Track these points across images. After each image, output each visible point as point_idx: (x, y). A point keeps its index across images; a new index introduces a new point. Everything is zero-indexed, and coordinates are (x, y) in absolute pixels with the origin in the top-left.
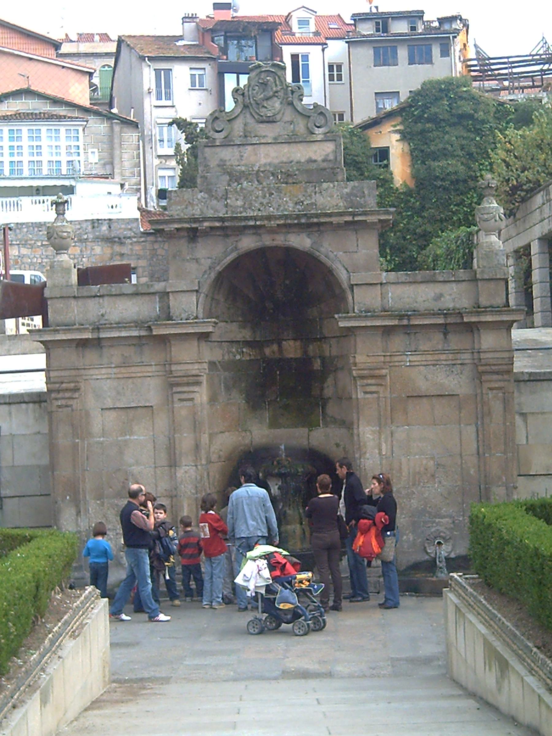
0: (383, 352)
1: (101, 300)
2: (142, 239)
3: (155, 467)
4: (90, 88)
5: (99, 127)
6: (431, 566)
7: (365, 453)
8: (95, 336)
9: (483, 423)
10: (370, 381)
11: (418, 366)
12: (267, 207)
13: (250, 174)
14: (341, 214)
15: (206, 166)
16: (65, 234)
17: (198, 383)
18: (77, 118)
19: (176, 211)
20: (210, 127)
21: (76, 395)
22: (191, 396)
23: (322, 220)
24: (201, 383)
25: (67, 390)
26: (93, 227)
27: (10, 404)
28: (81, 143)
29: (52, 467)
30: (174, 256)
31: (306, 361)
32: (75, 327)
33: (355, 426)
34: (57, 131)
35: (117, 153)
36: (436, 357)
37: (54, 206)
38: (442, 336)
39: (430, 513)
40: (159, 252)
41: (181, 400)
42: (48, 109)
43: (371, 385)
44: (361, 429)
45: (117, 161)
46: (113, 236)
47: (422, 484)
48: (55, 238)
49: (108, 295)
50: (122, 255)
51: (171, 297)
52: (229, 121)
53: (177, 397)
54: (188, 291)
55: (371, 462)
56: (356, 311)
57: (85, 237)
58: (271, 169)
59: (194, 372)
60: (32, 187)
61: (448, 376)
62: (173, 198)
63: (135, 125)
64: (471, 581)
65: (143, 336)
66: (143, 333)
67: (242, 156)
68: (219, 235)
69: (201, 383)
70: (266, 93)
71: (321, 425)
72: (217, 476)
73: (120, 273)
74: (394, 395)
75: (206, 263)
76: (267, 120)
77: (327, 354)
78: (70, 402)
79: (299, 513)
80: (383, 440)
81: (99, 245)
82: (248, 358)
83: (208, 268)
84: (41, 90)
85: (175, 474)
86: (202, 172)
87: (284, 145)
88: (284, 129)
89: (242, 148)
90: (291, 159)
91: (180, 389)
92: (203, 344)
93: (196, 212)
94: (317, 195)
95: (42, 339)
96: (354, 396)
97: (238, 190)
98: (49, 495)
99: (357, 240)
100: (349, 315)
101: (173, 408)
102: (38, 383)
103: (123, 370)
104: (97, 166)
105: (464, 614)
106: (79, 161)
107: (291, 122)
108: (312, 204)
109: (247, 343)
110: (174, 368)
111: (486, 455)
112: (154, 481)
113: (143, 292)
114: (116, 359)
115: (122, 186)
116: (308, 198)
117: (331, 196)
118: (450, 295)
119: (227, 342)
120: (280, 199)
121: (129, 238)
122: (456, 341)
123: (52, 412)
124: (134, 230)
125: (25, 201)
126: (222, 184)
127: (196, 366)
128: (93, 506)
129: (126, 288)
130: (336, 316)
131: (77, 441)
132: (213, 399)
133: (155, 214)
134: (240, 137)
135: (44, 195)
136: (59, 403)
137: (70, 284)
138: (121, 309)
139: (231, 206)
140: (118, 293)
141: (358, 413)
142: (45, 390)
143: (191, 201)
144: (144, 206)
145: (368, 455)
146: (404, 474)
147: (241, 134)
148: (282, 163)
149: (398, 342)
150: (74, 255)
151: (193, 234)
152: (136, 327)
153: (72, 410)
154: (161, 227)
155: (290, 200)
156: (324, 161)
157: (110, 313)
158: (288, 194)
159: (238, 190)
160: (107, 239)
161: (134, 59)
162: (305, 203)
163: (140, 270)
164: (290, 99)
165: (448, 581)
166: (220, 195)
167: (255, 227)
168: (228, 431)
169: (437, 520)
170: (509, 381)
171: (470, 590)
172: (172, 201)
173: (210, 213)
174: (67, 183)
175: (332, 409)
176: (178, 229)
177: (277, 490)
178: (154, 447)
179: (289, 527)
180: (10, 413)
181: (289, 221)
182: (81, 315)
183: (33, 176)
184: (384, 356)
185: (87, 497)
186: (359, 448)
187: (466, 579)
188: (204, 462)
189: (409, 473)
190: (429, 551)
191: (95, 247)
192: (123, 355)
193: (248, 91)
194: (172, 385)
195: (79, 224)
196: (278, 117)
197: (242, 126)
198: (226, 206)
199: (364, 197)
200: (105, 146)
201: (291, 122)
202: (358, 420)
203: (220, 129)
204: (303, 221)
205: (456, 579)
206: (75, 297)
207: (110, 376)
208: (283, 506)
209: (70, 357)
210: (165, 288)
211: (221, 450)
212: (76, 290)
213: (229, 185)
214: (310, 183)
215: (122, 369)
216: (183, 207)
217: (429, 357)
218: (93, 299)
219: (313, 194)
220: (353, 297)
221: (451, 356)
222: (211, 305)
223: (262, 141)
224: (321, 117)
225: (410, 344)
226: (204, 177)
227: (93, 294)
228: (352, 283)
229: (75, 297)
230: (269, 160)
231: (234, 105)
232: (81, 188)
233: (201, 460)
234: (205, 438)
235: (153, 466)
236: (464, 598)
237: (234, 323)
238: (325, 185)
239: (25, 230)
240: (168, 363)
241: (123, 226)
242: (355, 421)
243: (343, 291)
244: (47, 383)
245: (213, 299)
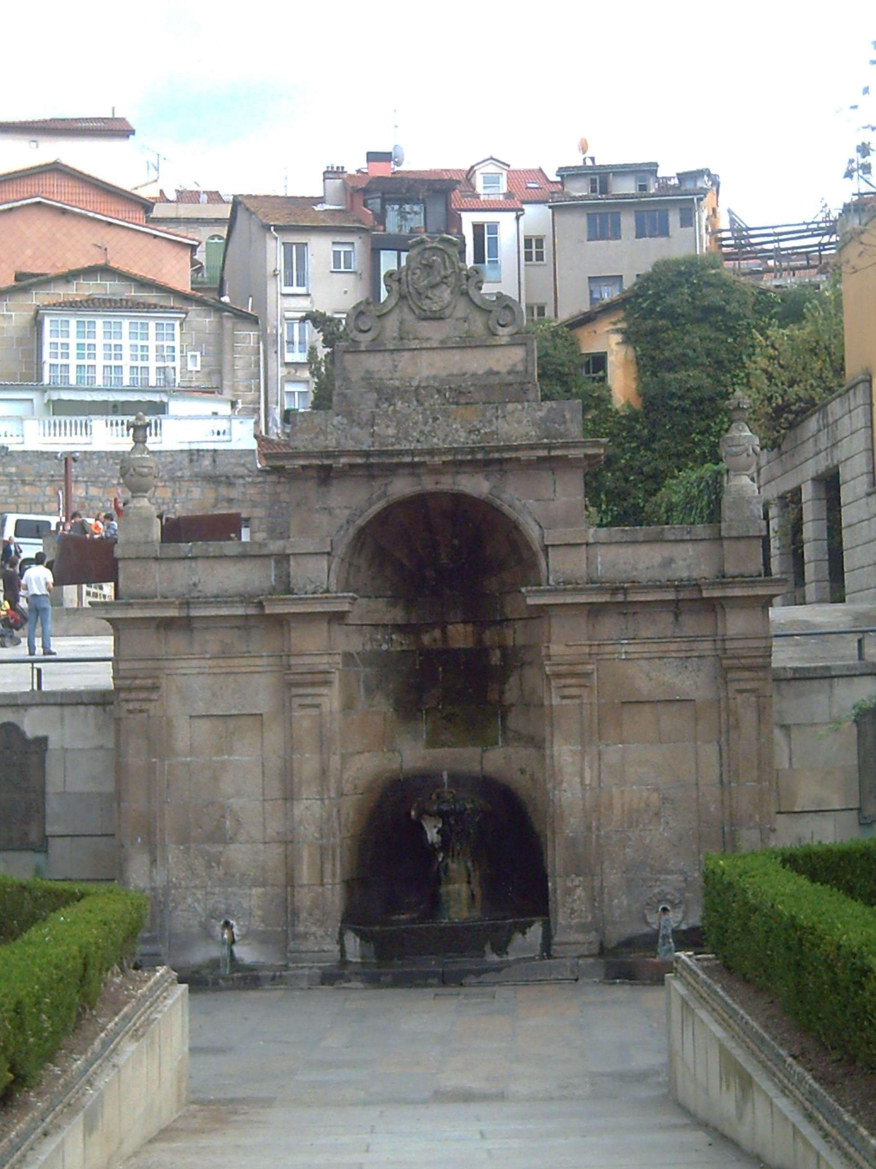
0: (589, 639)
1: (193, 564)
2: (260, 479)
3: (264, 800)
4: (192, 267)
5: (203, 321)
6: (650, 942)
7: (561, 782)
8: (183, 614)
9: (728, 740)
10: (569, 681)
11: (638, 659)
12: (430, 437)
13: (406, 391)
14: (531, 447)
15: (346, 379)
16: (146, 470)
17: (327, 683)
18: (172, 308)
19: (302, 442)
20: (352, 324)
21: (155, 696)
22: (317, 701)
23: (506, 455)
24: (331, 682)
25: (141, 688)
26: (191, 461)
27: (62, 705)
28: (177, 344)
29: (118, 796)
30: (298, 505)
31: (480, 652)
32: (156, 600)
33: (547, 745)
34: (145, 326)
35: (227, 357)
36: (663, 647)
37: (132, 431)
38: (671, 618)
39: (652, 868)
40: (284, 497)
41: (303, 706)
42: (133, 294)
43: (570, 686)
44: (555, 748)
45: (227, 369)
46: (218, 473)
47: (641, 826)
48: (132, 475)
49: (203, 557)
50: (230, 501)
51: (292, 563)
52: (379, 317)
53: (296, 702)
54: (316, 554)
55: (570, 795)
56: (551, 582)
57: (179, 474)
58: (436, 384)
59: (322, 668)
60: (107, 402)
61: (680, 673)
62: (299, 424)
63: (253, 320)
64: (705, 963)
65: (252, 615)
66: (251, 611)
67: (396, 366)
68: (361, 476)
69: (331, 682)
70: (430, 279)
71: (500, 743)
73: (224, 527)
74: (603, 701)
75: (342, 515)
76: (432, 316)
77: (510, 643)
78: (145, 706)
79: (467, 867)
80: (586, 764)
81: (198, 487)
82: (399, 649)
83: (345, 522)
84: (124, 269)
85: (292, 810)
86: (340, 388)
87: (454, 351)
88: (455, 329)
89: (396, 356)
90: (464, 370)
91: (301, 691)
92: (335, 627)
93: (331, 442)
94: (500, 420)
95: (109, 616)
96: (546, 703)
97: (390, 412)
98: (113, 835)
99: (555, 484)
100: (542, 588)
101: (291, 717)
102: (101, 677)
103: (222, 663)
104: (198, 374)
105: (693, 1010)
106: (174, 368)
107: (465, 320)
108: (493, 433)
109: (398, 628)
110: (293, 661)
111: (733, 785)
112: (262, 820)
113: (252, 553)
114: (213, 647)
115: (233, 404)
116: (487, 424)
117: (519, 422)
118: (685, 560)
119: (369, 625)
120: (448, 425)
121: (242, 477)
123: (120, 719)
124: (249, 466)
125: (98, 423)
126: (367, 405)
127: (325, 659)
129: (229, 547)
130: (523, 590)
131: (154, 760)
132: (348, 706)
133: (278, 444)
134: (394, 339)
135: (124, 415)
136: (131, 706)
137: (150, 540)
138: (222, 576)
139: (379, 435)
140: (217, 554)
141: (552, 725)
142: (113, 687)
143: (323, 428)
144: (263, 433)
145: (565, 785)
146: (615, 812)
147: (396, 335)
148: (452, 375)
149: (609, 626)
150: (164, 499)
151: (326, 475)
152: (242, 602)
153: (149, 716)
154: (281, 463)
155: (462, 427)
156: (509, 373)
157: (205, 582)
158: (459, 419)
159: (390, 412)
160: (210, 477)
161: (255, 229)
162: (482, 431)
163: (255, 523)
164: (465, 287)
165: (672, 963)
166: (365, 420)
167: (412, 465)
168: (369, 752)
169: (662, 877)
170: (765, 680)
171: (703, 976)
172: (297, 428)
173: (350, 445)
174: (156, 398)
175: (515, 721)
176: (303, 467)
177: (435, 835)
178: (263, 772)
179: (451, 887)
180: (62, 719)
181: (459, 457)
182: (165, 585)
183: (109, 387)
184: (590, 645)
185: (167, 842)
186: (553, 776)
187: (698, 960)
188: (333, 794)
189: (623, 811)
190: (650, 920)
191: (194, 489)
192: (222, 641)
193: (407, 275)
194: (291, 685)
195: (172, 455)
196: (447, 312)
197: (398, 324)
198: (372, 435)
199: (565, 422)
200: (211, 348)
201: (465, 320)
202: (552, 735)
203: (366, 328)
204: (479, 456)
205: (683, 961)
206: (156, 559)
207: (202, 670)
208: (443, 858)
209: (146, 643)
210: (285, 548)
211: (358, 778)
212: (158, 548)
213: (377, 406)
214: (490, 403)
215: (220, 660)
216: (312, 435)
217: (654, 647)
218: (182, 562)
219: (494, 419)
220: (547, 565)
221: (684, 646)
222: (348, 573)
223: (425, 345)
224: (507, 312)
225: (626, 628)
226: (343, 396)
227: (183, 554)
228: (546, 543)
229: (156, 559)
230: (433, 372)
231: (387, 294)
232: (176, 406)
233: (329, 790)
234: (335, 761)
235: (261, 798)
236: (694, 988)
237: (381, 599)
238: (510, 407)
239: (96, 462)
240: (283, 656)
241: (233, 461)
242: (548, 737)
243: (534, 555)
244: (114, 678)
245: (350, 565)
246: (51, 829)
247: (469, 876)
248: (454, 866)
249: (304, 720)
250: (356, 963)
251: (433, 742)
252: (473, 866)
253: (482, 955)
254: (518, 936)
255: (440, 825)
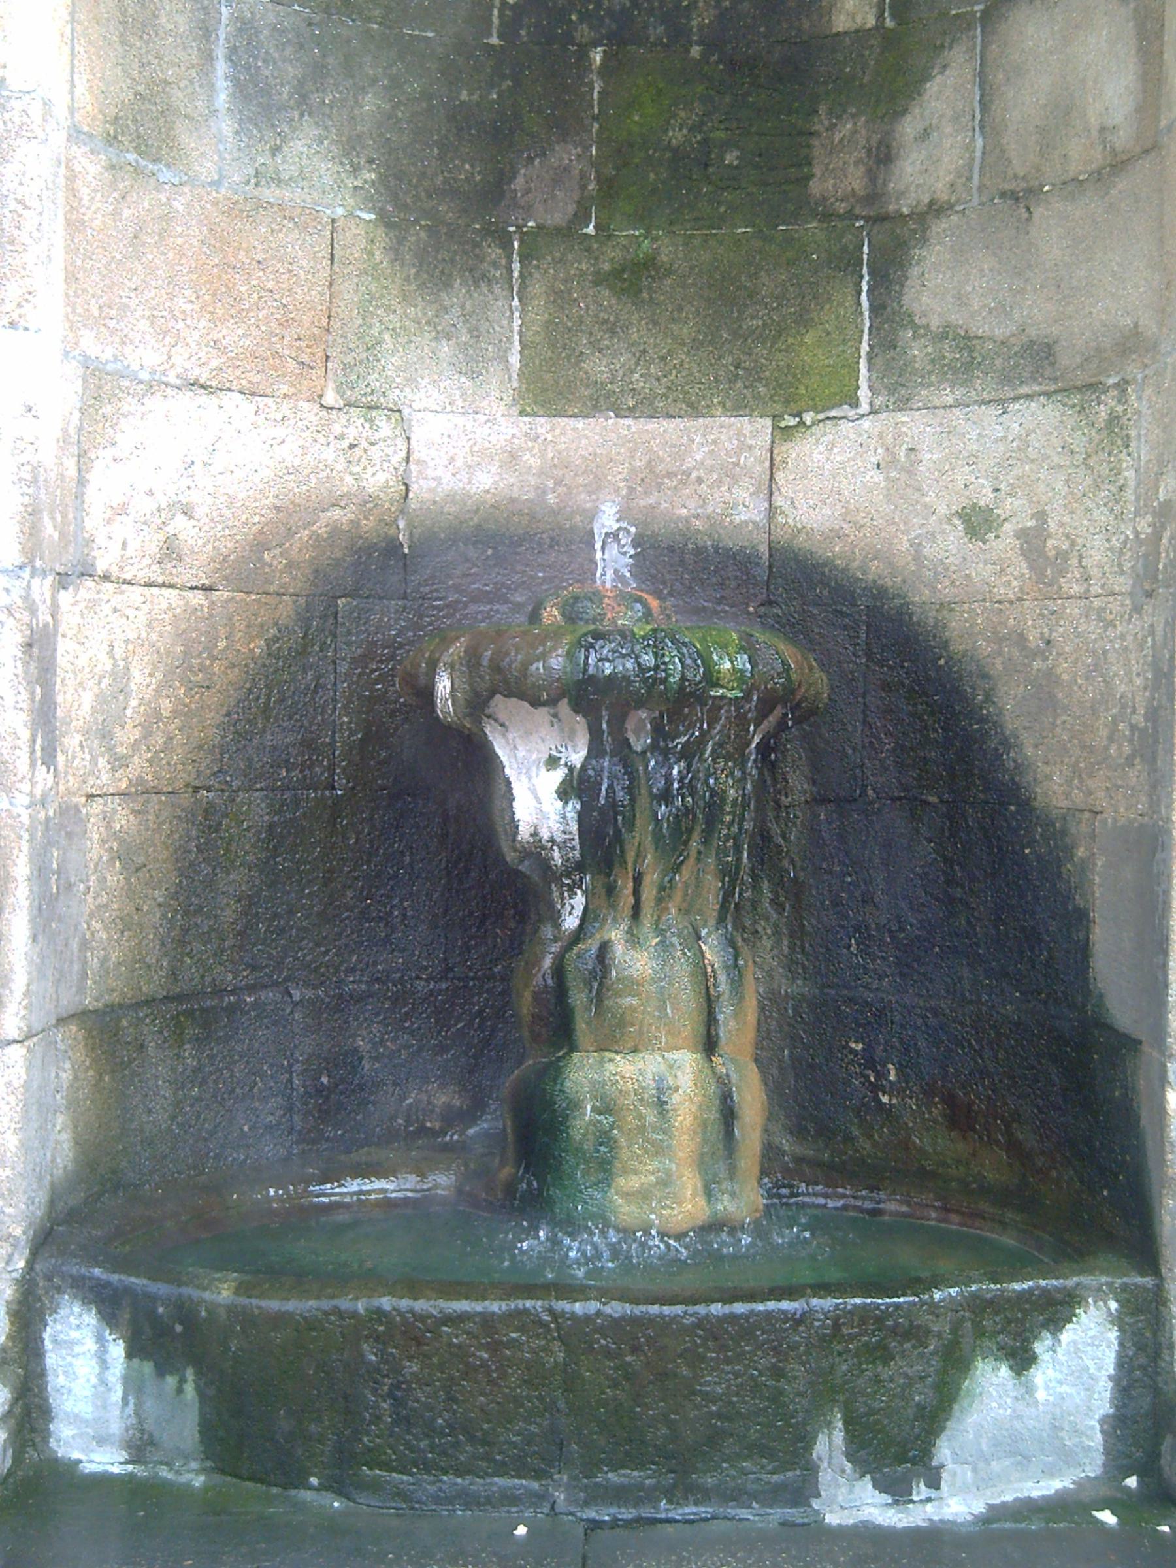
72: (141, 680)
247: (711, 1020)
248: (635, 961)
250: (103, 1480)
251: (550, 387)
252: (735, 970)
253: (803, 1490)
254: (991, 1380)
255: (577, 756)
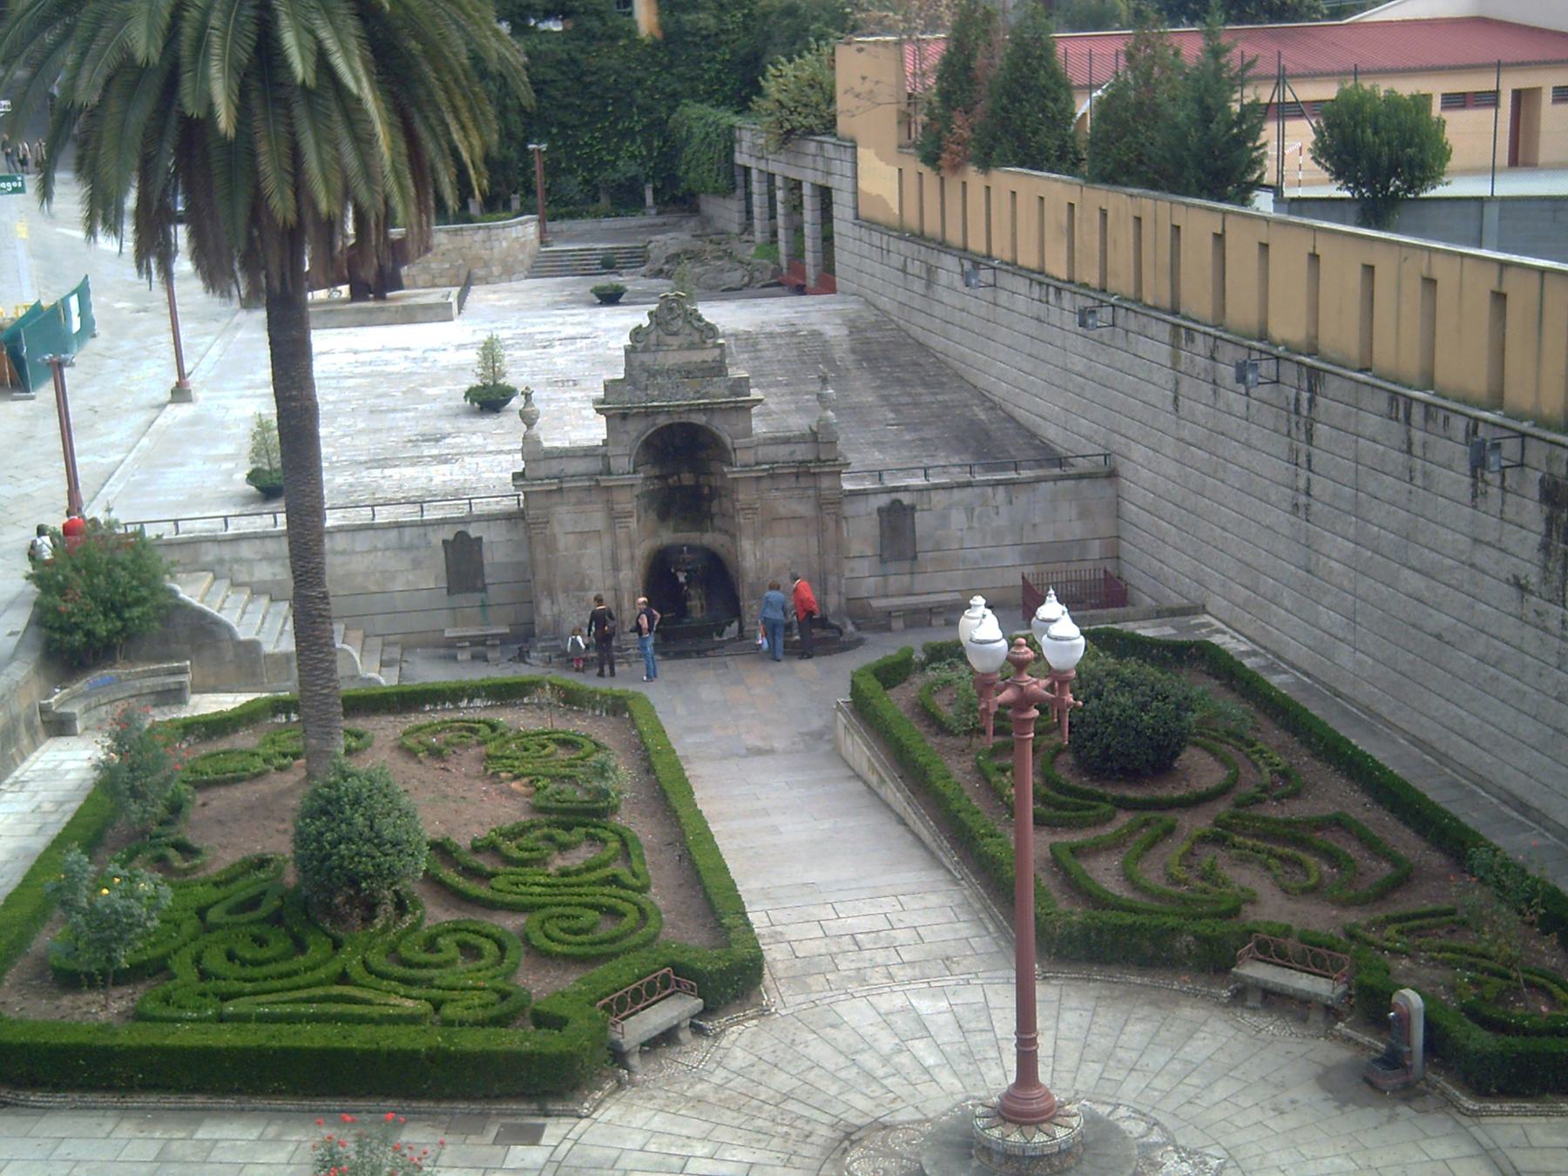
114: (573, 500)
122: (803, 482)
128: (561, 597)
246: (487, 581)
249: (621, 534)
